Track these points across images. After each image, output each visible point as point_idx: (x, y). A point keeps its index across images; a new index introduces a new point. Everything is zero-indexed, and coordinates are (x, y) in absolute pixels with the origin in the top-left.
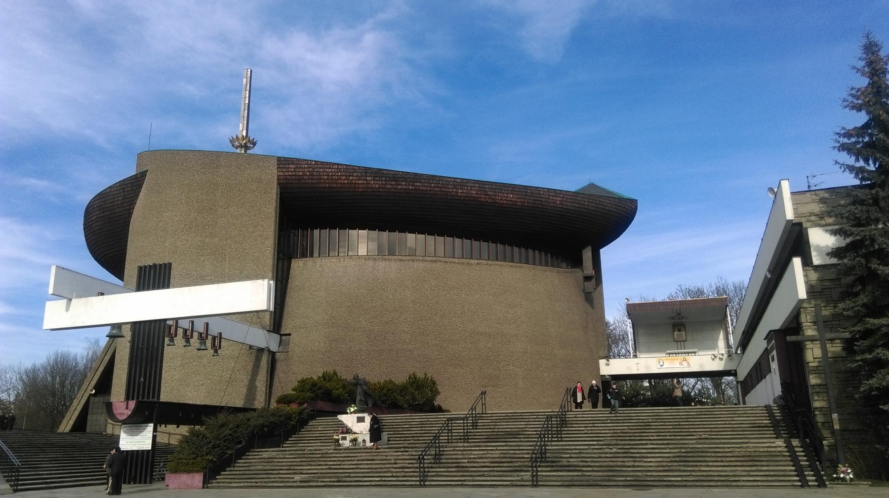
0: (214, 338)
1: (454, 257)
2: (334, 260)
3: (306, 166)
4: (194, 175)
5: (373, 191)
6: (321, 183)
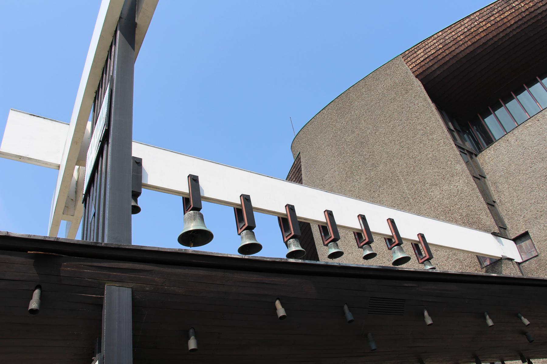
0: (416, 246)
2: (530, 124)
3: (435, 41)
4: (335, 126)
5: (531, 13)
6: (461, 46)
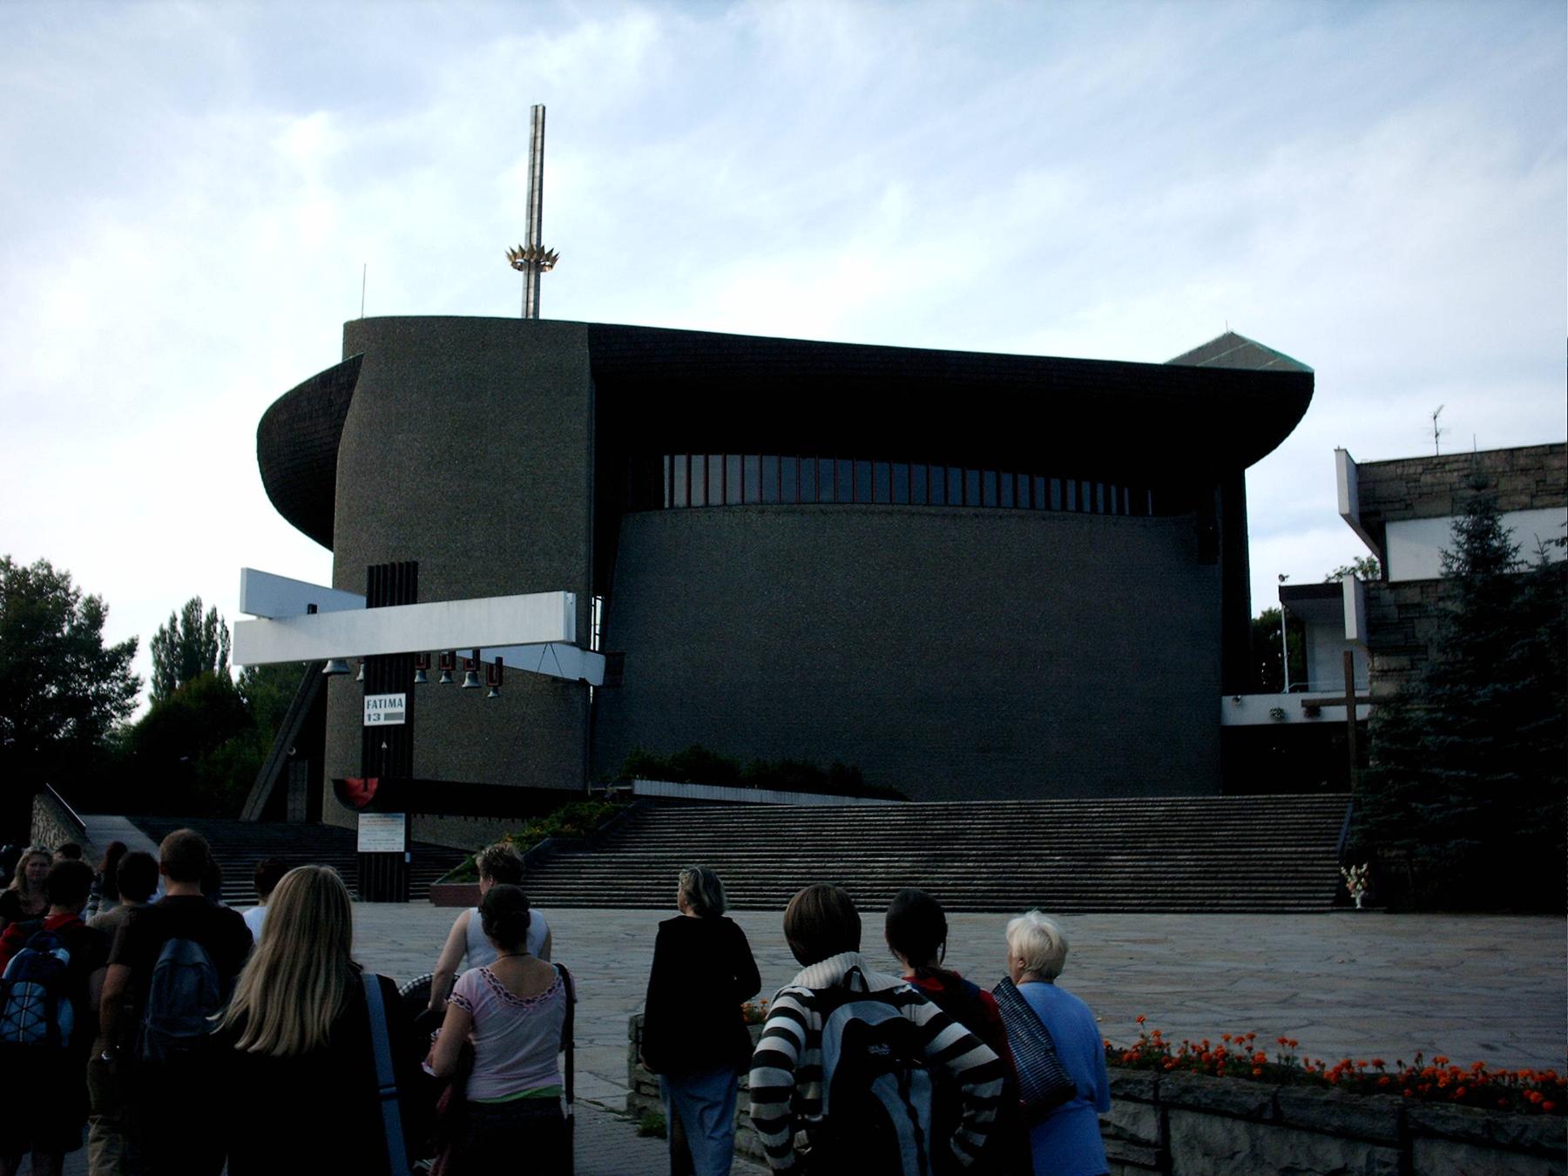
1: (928, 504)
